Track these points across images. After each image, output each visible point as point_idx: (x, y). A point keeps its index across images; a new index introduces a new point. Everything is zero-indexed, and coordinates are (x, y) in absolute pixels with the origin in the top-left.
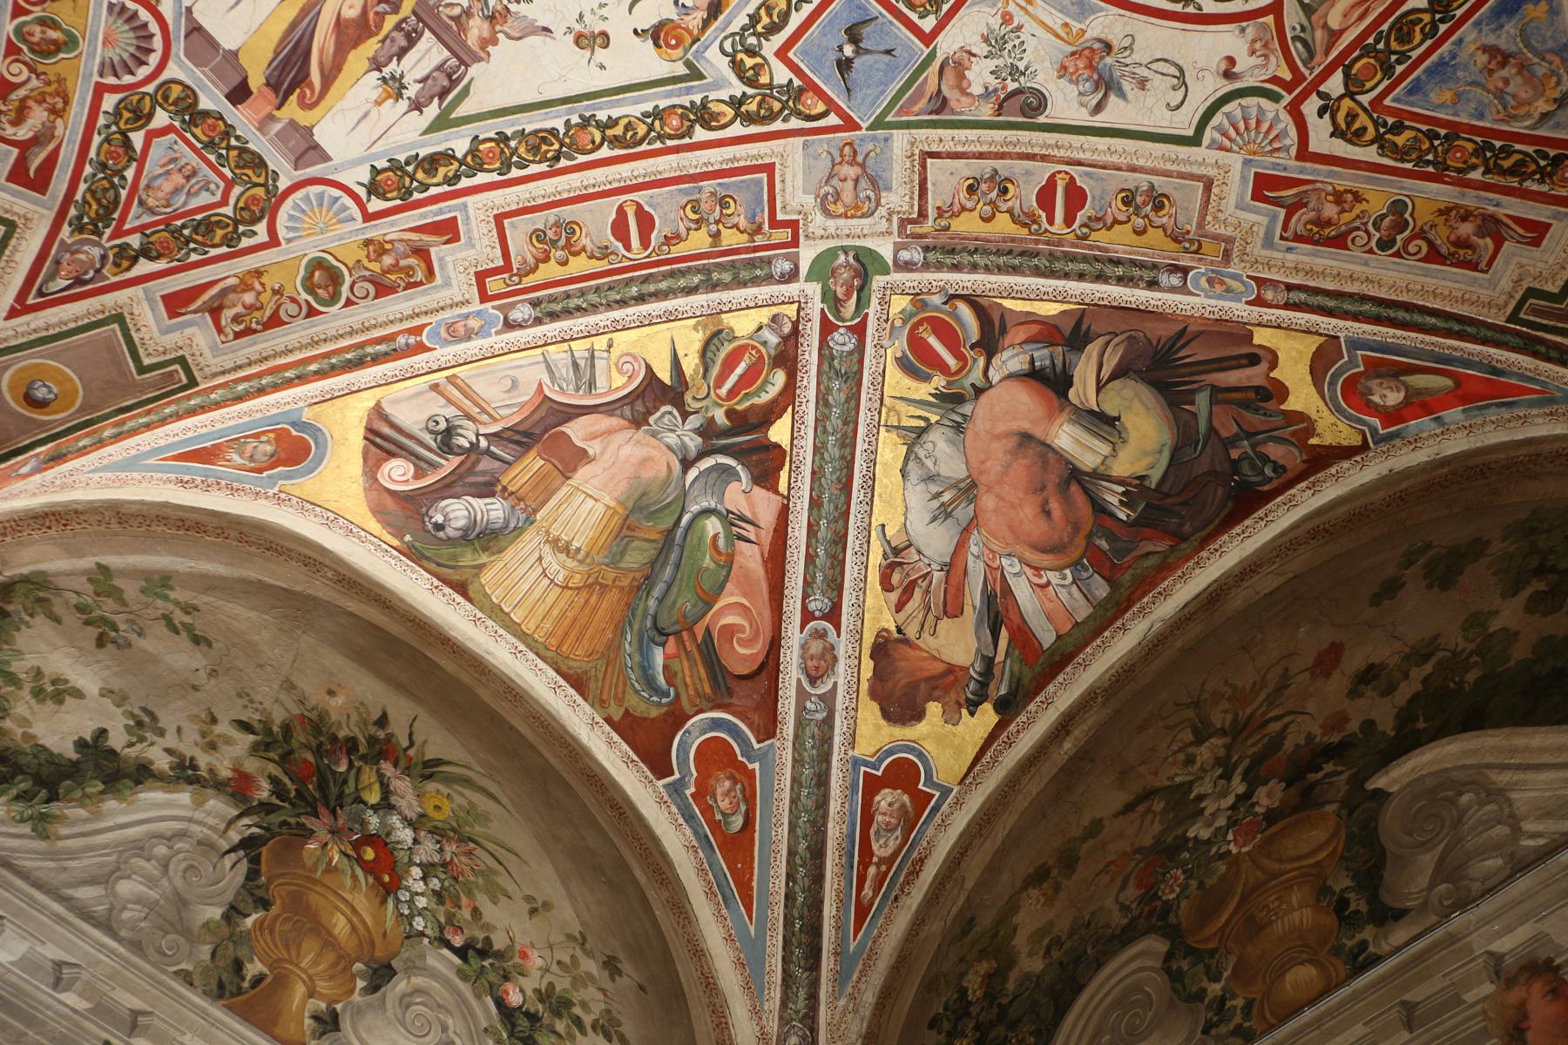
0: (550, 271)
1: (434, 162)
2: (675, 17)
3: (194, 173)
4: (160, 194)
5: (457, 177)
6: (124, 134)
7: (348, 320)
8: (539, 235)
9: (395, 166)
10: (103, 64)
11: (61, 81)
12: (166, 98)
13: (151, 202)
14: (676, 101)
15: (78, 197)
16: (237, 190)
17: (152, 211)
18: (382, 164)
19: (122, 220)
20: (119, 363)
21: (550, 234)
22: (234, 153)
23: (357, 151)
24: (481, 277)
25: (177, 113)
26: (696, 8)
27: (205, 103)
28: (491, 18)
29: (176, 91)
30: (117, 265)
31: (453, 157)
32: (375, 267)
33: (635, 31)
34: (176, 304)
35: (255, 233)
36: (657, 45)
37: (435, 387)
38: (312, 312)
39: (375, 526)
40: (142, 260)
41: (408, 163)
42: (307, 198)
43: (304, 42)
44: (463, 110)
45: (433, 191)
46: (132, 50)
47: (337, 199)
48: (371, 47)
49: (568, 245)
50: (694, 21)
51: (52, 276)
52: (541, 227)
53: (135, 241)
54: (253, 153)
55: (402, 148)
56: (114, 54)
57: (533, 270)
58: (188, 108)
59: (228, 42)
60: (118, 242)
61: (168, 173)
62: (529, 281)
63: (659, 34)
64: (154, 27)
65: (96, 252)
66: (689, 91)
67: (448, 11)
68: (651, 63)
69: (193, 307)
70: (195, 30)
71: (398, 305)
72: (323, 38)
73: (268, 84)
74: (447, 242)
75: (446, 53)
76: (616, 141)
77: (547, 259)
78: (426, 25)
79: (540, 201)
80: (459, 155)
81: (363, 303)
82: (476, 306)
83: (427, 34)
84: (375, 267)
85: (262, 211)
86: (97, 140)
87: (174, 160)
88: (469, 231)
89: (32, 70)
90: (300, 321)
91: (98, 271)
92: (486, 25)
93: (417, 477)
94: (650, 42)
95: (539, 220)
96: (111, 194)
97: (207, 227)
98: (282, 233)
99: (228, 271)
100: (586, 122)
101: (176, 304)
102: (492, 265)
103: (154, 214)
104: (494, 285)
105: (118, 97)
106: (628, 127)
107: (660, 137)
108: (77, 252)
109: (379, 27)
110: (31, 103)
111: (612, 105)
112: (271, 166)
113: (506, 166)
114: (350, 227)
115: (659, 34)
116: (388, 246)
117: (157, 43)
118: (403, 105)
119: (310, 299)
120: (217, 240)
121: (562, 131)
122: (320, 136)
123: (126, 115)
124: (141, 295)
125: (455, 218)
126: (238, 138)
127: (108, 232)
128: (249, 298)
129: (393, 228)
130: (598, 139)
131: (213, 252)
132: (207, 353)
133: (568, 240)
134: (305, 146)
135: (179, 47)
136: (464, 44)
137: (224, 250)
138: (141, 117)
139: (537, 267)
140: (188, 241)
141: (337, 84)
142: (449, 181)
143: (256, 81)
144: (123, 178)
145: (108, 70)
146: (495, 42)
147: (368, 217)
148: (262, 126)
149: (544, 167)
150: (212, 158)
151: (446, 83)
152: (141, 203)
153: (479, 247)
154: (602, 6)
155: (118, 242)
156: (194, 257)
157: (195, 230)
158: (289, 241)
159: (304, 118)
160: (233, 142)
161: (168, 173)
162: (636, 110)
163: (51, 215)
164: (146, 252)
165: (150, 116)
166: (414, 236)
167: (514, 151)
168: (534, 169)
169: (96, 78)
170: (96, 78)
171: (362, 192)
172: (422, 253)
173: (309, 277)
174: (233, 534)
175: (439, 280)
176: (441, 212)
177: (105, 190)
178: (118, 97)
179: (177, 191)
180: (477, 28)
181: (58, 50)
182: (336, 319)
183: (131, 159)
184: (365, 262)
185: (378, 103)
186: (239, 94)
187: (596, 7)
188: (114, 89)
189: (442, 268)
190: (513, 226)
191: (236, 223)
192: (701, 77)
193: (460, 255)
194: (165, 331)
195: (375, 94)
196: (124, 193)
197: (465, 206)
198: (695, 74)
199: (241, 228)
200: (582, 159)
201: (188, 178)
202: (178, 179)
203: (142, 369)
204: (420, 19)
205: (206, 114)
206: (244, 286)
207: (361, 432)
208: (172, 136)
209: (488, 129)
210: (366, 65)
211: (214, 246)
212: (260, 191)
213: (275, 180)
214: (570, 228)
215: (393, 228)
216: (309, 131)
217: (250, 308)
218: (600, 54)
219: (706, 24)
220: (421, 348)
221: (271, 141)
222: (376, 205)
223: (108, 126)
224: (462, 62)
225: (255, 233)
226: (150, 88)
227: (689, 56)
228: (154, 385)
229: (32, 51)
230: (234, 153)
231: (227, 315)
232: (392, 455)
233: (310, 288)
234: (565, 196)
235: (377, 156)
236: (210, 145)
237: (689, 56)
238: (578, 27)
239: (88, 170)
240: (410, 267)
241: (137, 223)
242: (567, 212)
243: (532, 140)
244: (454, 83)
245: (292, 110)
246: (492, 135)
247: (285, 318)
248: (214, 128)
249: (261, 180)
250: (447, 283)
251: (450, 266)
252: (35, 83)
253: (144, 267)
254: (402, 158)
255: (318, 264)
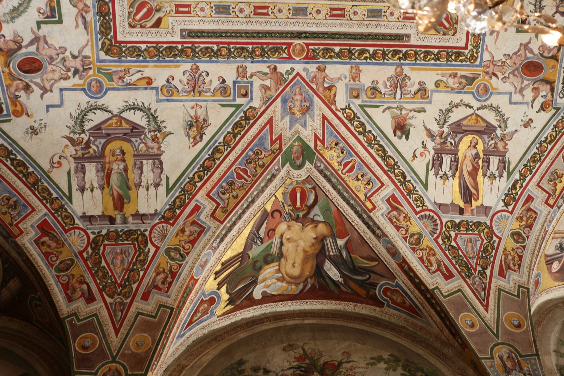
0: (559, 187)
1: (514, 186)
2: (544, 100)
3: (471, 240)
4: (471, 252)
5: (522, 184)
6: (450, 245)
7: (532, 243)
8: (550, 180)
9: (507, 195)
10: (430, 233)
11: (428, 246)
12: (449, 228)
13: (471, 256)
14: (557, 120)
15: (460, 270)
16: (482, 234)
17: (473, 258)
18: (503, 197)
19: (472, 266)
20: (514, 300)
21: (552, 178)
22: (473, 226)
23: (496, 200)
24: (546, 202)
25: (454, 229)
26: (547, 94)
27: (457, 221)
28: (502, 140)
29: (449, 224)
30: (484, 277)
31: (518, 180)
32: (524, 223)
33: (537, 112)
34: (502, 274)
35: (495, 241)
36: (544, 110)
37: (553, 238)
38: (524, 247)
39: (557, 283)
40: (486, 271)
41: (509, 192)
42: (496, 222)
43: (465, 185)
44: (511, 168)
45: (519, 193)
46: (432, 224)
47: (502, 215)
48: (480, 172)
49: (558, 177)
50: (549, 97)
51: (480, 295)
52: (548, 178)
53: (479, 268)
54: (476, 222)
55: (505, 190)
56: (430, 228)
57: (556, 190)
58: (456, 226)
59: (449, 202)
60: (477, 272)
61: (467, 245)
62: (557, 193)
63: (543, 108)
64: (432, 214)
65: (477, 279)
66: (559, 115)
67: (491, 147)
68: (545, 116)
69: (505, 271)
70: (440, 206)
71: (537, 227)
72: (469, 181)
73: (465, 203)
74: (532, 202)
75: (498, 158)
76: (550, 142)
77: (556, 185)
78: (489, 155)
79: (544, 172)
80: (518, 179)
81: (530, 234)
82: (552, 210)
83: (490, 157)
84: (524, 223)
85: (491, 234)
86: (447, 252)
87: (465, 241)
88: (534, 194)
89: (421, 250)
90: (525, 252)
91: (483, 283)
92: (502, 142)
93: (560, 263)
94: (542, 111)
95: (547, 177)
96: (463, 262)
97: (486, 250)
98: (499, 235)
99: (500, 255)
100: (541, 144)
101: (502, 274)
102: (546, 198)
103: (475, 258)
104: (551, 202)
105: (440, 238)
106: (551, 137)
107: (560, 131)
108: (475, 284)
109: (479, 166)
110: (428, 258)
111: (543, 134)
112: (482, 221)
113: (531, 171)
114: (510, 219)
115: (543, 108)
116: (521, 215)
117: (435, 217)
118: (498, 179)
119: (520, 244)
120: (491, 251)
121: (537, 151)
122: (486, 204)
123: (446, 240)
124: (495, 279)
125: (529, 195)
126: (470, 222)
127: (473, 271)
128: (510, 257)
129: (519, 210)
130: (546, 145)
131: (493, 254)
132: (521, 279)
133: (557, 175)
134: (484, 210)
135: (440, 213)
136: (500, 152)
137: (494, 251)
138: (449, 238)
139: (556, 189)
140: (486, 256)
141: (479, 188)
142: (521, 187)
143: (462, 205)
144: (461, 256)
145: (433, 234)
146: (507, 145)
147: (511, 213)
148: (473, 214)
149: (539, 163)
150: (470, 232)
151: (503, 165)
152: (470, 258)
153: (539, 196)
154: (525, 113)
155: (477, 272)
156: (492, 259)
157: (485, 253)
158: (502, 235)
159: (478, 203)
160: (471, 224)
161: (467, 245)
162: (550, 130)
163: (461, 280)
164: (484, 269)
165: (450, 235)
166: (524, 208)
167: (530, 166)
168: (537, 166)
169: (432, 238)
170: (432, 238)
171: (505, 208)
172: (529, 210)
173: (514, 240)
174: (542, 316)
175: (539, 212)
176: (525, 196)
177: (461, 262)
178: (440, 238)
179: (472, 247)
180: (500, 145)
181: (420, 240)
182: (530, 243)
183: (457, 250)
184: (521, 224)
185: (492, 184)
186: (461, 211)
187: (523, 115)
188: (438, 237)
189: (536, 209)
190: (543, 184)
191: (489, 242)
192: (560, 108)
193: (537, 202)
194: (509, 283)
195: (490, 183)
196: (465, 259)
197: (529, 189)
198: (558, 109)
199: (491, 242)
200: (546, 153)
201: (471, 242)
202: (470, 244)
203: (519, 297)
204: (486, 155)
205: (460, 223)
206: (506, 256)
207: (545, 264)
208: (459, 236)
209: (521, 167)
210: (482, 177)
211: (492, 252)
212: (486, 230)
213: (486, 224)
214: (555, 172)
215: (519, 210)
216: (482, 205)
217: (513, 259)
218: (532, 125)
219: (552, 95)
220: (547, 231)
221: (477, 215)
222: (510, 208)
223: (446, 247)
224: (503, 156)
225: (495, 241)
226: (444, 229)
227: (554, 106)
228: (524, 298)
229: (416, 245)
230: (473, 226)
231: (511, 265)
232: (552, 263)
233: (517, 242)
234: (548, 166)
235: (501, 197)
236: (467, 230)
237: (554, 106)
238: (523, 123)
239: (454, 261)
240: (530, 216)
241: (475, 263)
242: (552, 169)
243: (532, 160)
244: (505, 163)
245: (475, 204)
246: (523, 167)
247: (521, 254)
248: (464, 225)
249: (484, 227)
250: (541, 212)
251: (538, 207)
252: (424, 252)
253: (488, 272)
254: (506, 192)
255: (513, 235)
